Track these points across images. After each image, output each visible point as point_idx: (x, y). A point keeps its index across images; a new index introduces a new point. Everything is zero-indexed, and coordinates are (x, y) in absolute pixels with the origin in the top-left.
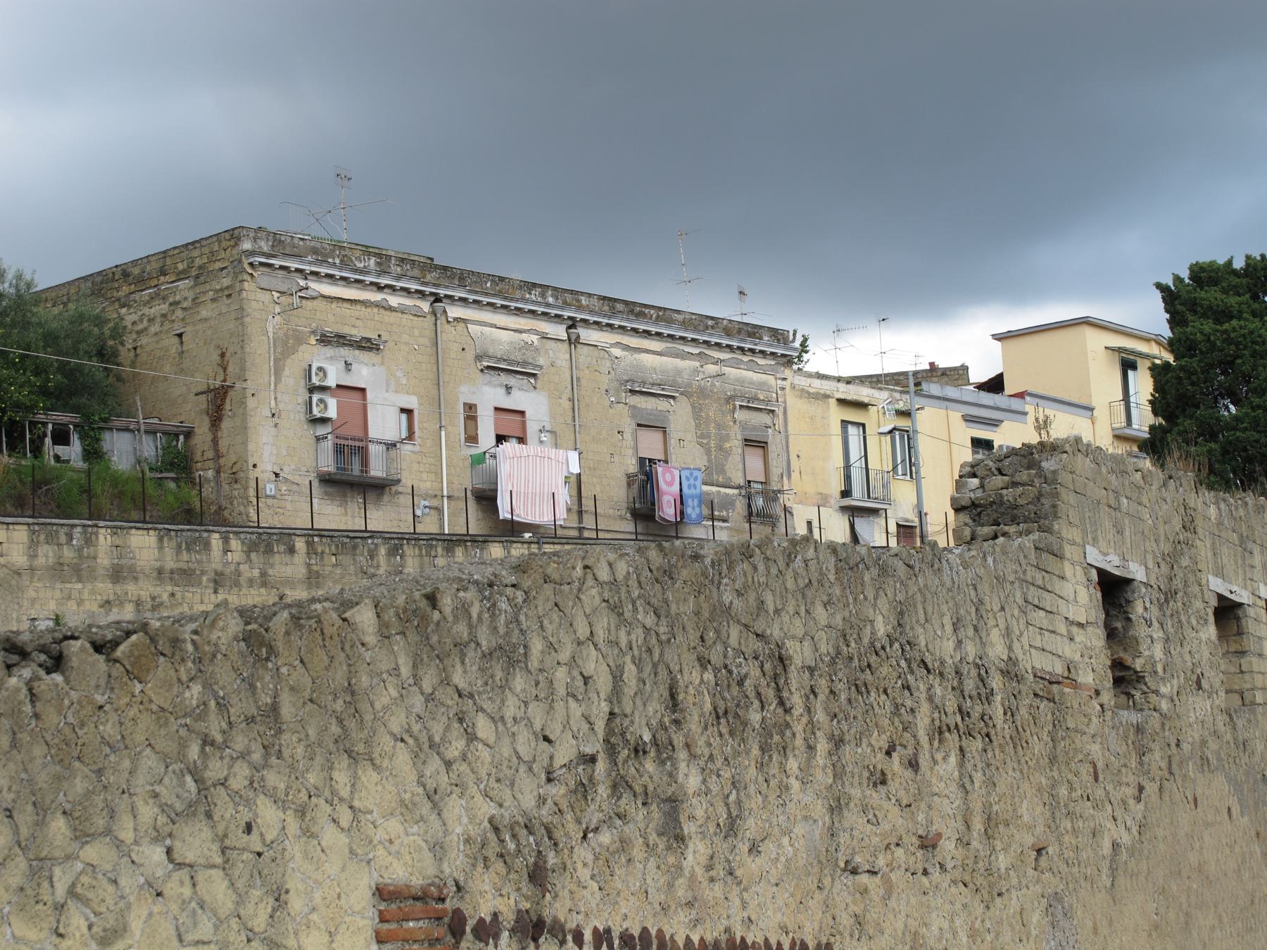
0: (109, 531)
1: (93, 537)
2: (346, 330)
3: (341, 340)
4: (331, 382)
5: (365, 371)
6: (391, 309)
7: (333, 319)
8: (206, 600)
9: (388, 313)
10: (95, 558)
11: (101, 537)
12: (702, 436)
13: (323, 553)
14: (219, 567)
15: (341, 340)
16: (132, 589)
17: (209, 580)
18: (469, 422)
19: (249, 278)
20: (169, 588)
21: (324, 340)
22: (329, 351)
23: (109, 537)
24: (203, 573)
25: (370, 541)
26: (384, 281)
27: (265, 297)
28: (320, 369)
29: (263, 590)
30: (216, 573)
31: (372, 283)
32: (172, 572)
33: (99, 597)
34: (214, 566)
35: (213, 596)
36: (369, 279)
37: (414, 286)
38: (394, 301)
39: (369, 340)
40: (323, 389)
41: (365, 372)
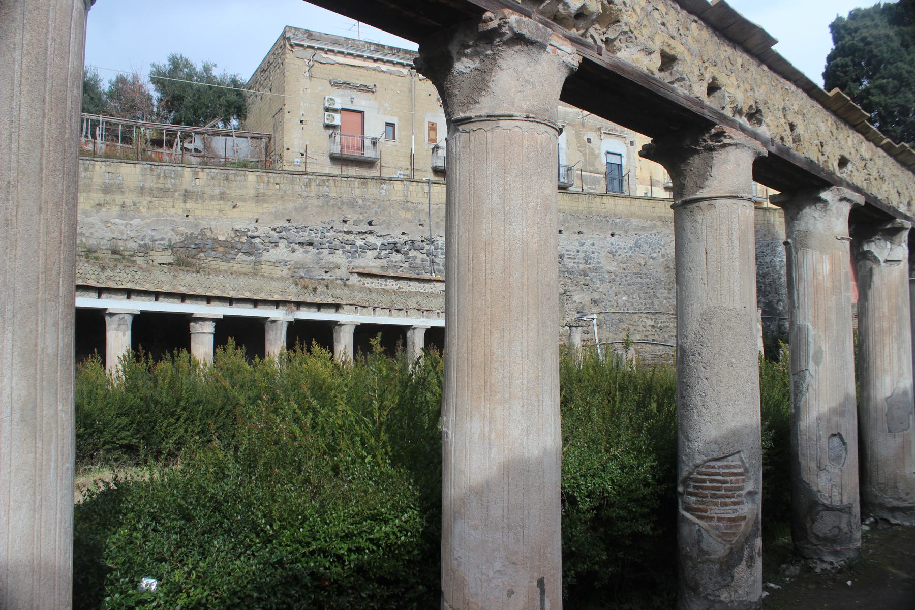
0: (103, 163)
1: (91, 167)
2: (351, 81)
3: (346, 85)
4: (338, 106)
5: (364, 103)
6: (383, 71)
7: (343, 75)
8: (177, 206)
9: (382, 74)
10: (91, 179)
11: (97, 167)
12: (581, 147)
13: (268, 182)
14: (189, 188)
15: (346, 85)
16: (119, 199)
17: (180, 195)
18: (431, 132)
19: (290, 52)
20: (149, 199)
21: (336, 84)
22: (340, 91)
23: (103, 167)
24: (175, 191)
25: (305, 177)
26: (376, 56)
27: (301, 62)
28: (332, 99)
29: (221, 202)
30: (186, 191)
31: (368, 58)
32: (151, 189)
33: (92, 202)
34: (184, 187)
35: (182, 205)
36: (366, 55)
37: (396, 60)
38: (384, 67)
39: (365, 86)
40: (335, 111)
41: (361, 102)
